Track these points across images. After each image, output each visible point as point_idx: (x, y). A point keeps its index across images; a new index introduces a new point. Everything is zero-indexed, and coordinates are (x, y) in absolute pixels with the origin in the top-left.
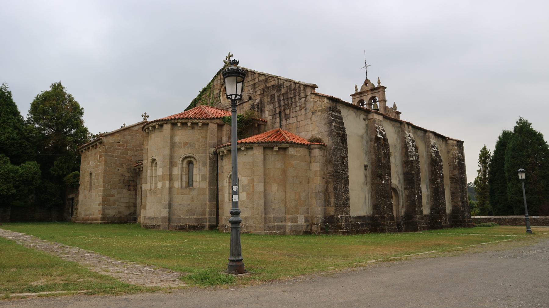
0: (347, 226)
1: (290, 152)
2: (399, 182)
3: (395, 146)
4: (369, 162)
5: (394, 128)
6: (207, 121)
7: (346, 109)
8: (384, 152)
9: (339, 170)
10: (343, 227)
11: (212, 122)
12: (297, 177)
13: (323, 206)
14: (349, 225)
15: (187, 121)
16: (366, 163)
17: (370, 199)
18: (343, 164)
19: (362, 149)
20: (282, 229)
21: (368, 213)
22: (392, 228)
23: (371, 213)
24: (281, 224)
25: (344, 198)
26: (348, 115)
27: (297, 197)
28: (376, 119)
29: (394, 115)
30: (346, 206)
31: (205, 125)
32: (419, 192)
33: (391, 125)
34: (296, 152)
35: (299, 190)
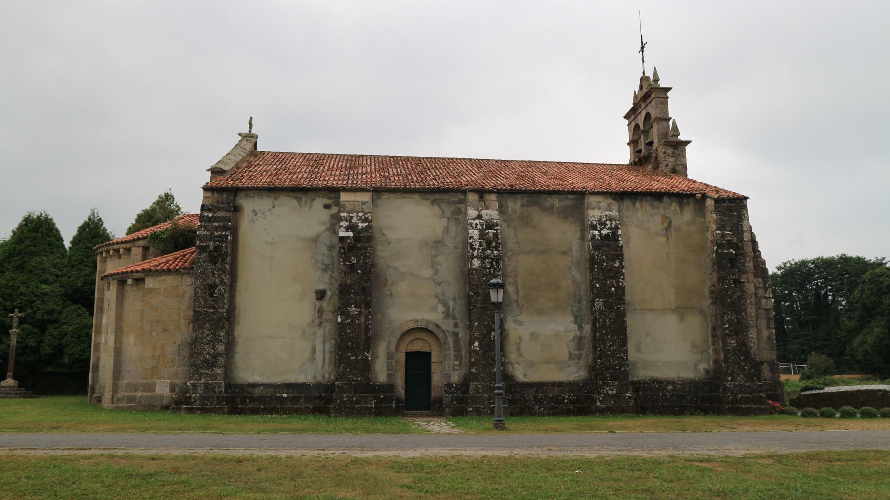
0: (203, 398)
1: (147, 284)
2: (447, 315)
3: (438, 243)
4: (332, 285)
5: (439, 206)
6: (128, 245)
7: (269, 197)
8: (349, 261)
9: (198, 307)
10: (193, 400)
11: (134, 246)
12: (158, 322)
13: (185, 366)
14: (212, 397)
15: (109, 249)
16: (321, 287)
17: (331, 352)
18: (211, 295)
19: (314, 261)
20: (133, 401)
21: (319, 379)
22: (355, 407)
23: (330, 378)
24: (133, 394)
25: (208, 353)
26: (274, 207)
27: (158, 353)
28: (346, 203)
29: (663, 150)
30: (212, 367)
31: (128, 250)
33: (428, 202)
34: (159, 283)
35: (163, 342)
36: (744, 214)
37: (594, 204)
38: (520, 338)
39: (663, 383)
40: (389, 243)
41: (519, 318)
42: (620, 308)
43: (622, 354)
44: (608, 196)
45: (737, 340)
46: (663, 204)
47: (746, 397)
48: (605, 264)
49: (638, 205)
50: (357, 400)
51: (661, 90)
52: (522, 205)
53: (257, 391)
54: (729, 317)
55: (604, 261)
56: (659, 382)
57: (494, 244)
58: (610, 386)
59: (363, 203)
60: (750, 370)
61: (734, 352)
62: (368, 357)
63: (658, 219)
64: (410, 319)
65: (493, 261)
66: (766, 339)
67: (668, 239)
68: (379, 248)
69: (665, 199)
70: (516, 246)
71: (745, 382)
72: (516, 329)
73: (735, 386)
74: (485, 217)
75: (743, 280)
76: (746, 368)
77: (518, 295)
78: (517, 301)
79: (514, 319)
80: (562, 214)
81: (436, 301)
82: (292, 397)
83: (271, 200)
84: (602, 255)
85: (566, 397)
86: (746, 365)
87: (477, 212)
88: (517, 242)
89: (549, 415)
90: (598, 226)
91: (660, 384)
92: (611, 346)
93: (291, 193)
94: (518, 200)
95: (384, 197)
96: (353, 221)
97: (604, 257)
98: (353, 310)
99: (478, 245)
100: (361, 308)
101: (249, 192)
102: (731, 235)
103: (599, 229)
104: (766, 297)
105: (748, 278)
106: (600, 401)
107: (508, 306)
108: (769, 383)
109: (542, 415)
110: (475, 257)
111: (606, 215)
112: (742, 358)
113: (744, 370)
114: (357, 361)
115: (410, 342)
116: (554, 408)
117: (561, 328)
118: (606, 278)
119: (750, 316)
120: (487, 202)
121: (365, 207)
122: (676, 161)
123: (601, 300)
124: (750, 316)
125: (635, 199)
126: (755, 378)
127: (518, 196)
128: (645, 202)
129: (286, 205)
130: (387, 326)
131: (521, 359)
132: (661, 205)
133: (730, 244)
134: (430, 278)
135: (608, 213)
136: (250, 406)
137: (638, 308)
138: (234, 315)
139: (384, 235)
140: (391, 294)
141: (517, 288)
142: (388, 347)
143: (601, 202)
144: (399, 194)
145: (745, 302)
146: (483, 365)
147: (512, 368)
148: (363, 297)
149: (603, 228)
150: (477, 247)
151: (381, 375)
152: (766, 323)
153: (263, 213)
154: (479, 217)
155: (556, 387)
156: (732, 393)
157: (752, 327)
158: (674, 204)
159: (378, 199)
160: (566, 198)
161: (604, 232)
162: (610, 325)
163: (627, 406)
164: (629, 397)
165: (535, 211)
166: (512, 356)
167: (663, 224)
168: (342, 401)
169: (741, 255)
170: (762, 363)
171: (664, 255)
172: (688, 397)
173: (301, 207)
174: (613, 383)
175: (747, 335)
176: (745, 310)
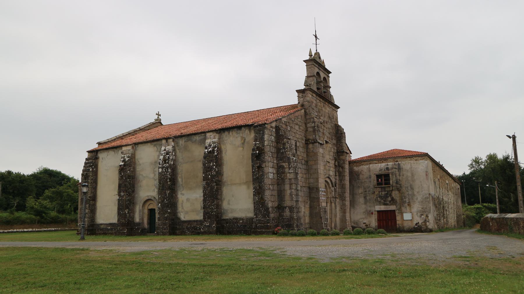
7: (106, 152)
8: (121, 175)
26: (108, 155)
32: (164, 200)
33: (153, 146)
36: (265, 132)
37: (209, 137)
38: (183, 201)
39: (238, 219)
40: (140, 165)
41: (183, 192)
42: (212, 185)
43: (212, 207)
44: (214, 132)
45: (258, 197)
46: (242, 131)
47: (261, 226)
48: (207, 165)
49: (231, 133)
50: (122, 229)
51: (309, 61)
52: (185, 142)
53: (102, 226)
54: (255, 186)
55: (206, 163)
56: (236, 219)
57: (167, 161)
58: (206, 222)
59: (129, 150)
60: (264, 212)
61: (257, 203)
62: (126, 212)
63: (239, 139)
64: (146, 196)
65: (166, 169)
66: (289, 195)
67: (243, 148)
68: (137, 167)
69: (243, 129)
70: (182, 160)
71: (262, 218)
72: (181, 197)
73: (257, 220)
74: (167, 150)
75: (263, 166)
76: (262, 211)
77: (182, 182)
78: (182, 185)
79: (181, 193)
80: (199, 143)
81: (155, 187)
82: (111, 228)
83: (107, 153)
84: (206, 161)
85: (198, 227)
86: (262, 210)
87: (165, 148)
88: (182, 159)
89: (191, 235)
90: (208, 147)
91: (236, 220)
92: (208, 203)
93: (112, 149)
94: (183, 139)
95: (139, 146)
96: (125, 158)
97: (206, 161)
98: (122, 194)
99: (161, 162)
100: (124, 193)
101: (101, 151)
102: (259, 143)
103: (208, 148)
104: (289, 173)
105: (266, 165)
106: (202, 228)
107: (178, 187)
108: (287, 218)
109: (189, 235)
110: (160, 168)
111: (212, 142)
112: (261, 206)
113: (261, 212)
114: (123, 213)
115: (149, 205)
116: (193, 232)
117: (198, 196)
118: (207, 171)
119: (266, 184)
120: (169, 143)
121: (129, 151)
122: (304, 100)
123: (205, 182)
124: (266, 184)
125: (230, 131)
126: (266, 216)
127: (183, 138)
128: (234, 131)
129: (111, 153)
130: (139, 199)
131: (183, 210)
132: (241, 132)
133: (258, 148)
134: (153, 178)
135: (214, 140)
136: (99, 232)
137: (229, 183)
138: (97, 198)
139: (139, 162)
140: (140, 186)
141: (182, 179)
142: (139, 208)
143: (211, 135)
144: (144, 144)
145: (264, 177)
146: (162, 214)
147: (180, 215)
148: (125, 188)
149: (210, 148)
150: (161, 163)
151: (137, 219)
152: (289, 186)
153: (105, 158)
154: (165, 150)
155: (195, 223)
156: (255, 224)
157: (267, 190)
158: (247, 130)
159: (137, 147)
160: (201, 135)
161: (209, 150)
162: (208, 194)
163: (212, 231)
164: (214, 226)
165: (189, 143)
166: (180, 209)
167: (241, 141)
168: (117, 230)
169: (263, 153)
170: (286, 207)
171: (241, 157)
172: (248, 226)
173: (115, 154)
174: (208, 220)
175: (264, 194)
176: (264, 181)
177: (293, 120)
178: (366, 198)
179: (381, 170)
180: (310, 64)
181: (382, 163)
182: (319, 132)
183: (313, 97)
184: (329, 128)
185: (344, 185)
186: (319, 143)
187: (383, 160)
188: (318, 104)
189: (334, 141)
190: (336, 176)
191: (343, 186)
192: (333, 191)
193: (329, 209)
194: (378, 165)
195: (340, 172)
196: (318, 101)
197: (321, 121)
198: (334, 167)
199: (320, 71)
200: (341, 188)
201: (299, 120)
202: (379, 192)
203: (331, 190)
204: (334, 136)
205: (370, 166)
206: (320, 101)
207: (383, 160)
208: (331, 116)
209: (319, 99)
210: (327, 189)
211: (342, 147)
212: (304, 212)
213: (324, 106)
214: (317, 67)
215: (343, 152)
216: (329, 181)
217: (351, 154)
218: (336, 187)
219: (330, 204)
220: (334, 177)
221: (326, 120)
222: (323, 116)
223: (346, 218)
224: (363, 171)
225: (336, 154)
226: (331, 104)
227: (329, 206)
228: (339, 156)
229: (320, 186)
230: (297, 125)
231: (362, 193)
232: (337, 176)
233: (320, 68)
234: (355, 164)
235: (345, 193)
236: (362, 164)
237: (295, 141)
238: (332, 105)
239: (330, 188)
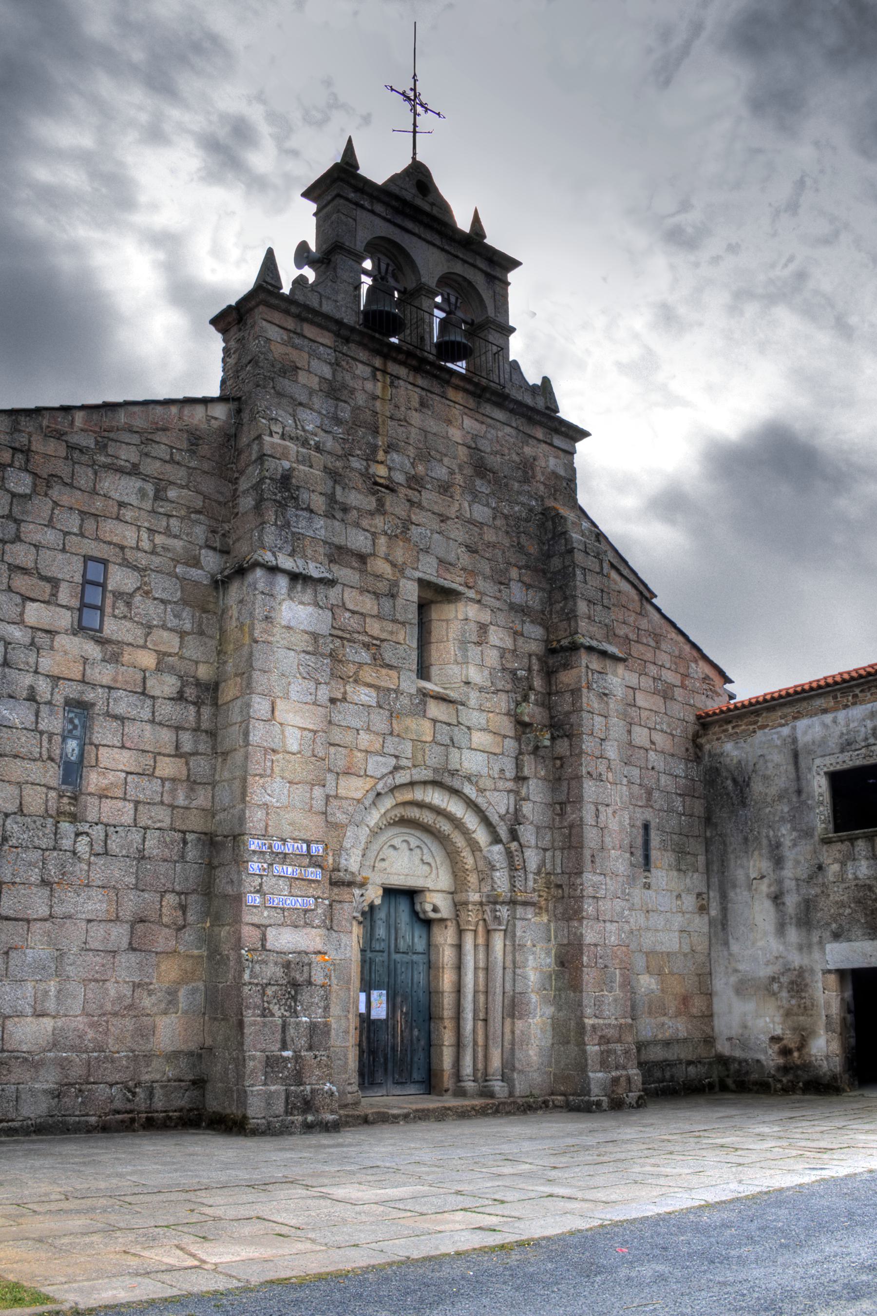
177: (88, 441)
178: (784, 904)
179: (847, 745)
180: (329, 198)
181: (854, 704)
182: (305, 514)
183: (297, 341)
184: (472, 522)
185: (574, 831)
186: (274, 570)
187: (857, 691)
188: (351, 383)
189: (533, 599)
190: (520, 779)
191: (570, 834)
192: (493, 868)
193: (476, 969)
194: (835, 721)
195: (561, 758)
196: (362, 370)
197: (382, 471)
198: (512, 734)
199: (415, 239)
200: (563, 849)
201: (161, 451)
202: (843, 864)
203: (485, 858)
204: (520, 568)
205: (794, 728)
206: (384, 372)
207: (858, 686)
208: (494, 461)
209: (378, 362)
210: (458, 853)
211: (573, 623)
212: (136, 986)
213: (423, 404)
214: (372, 212)
215: (574, 647)
216: (456, 808)
217: (731, 681)
218: (514, 846)
219: (481, 941)
220: (510, 785)
221: (440, 472)
222: (412, 452)
223: (582, 1017)
224: (766, 762)
225: (534, 660)
226: (500, 405)
227: (476, 946)
228: (549, 674)
229: (255, 819)
230: (129, 474)
231: (763, 877)
232: (525, 779)
233: (410, 225)
234: (730, 727)
235: (580, 873)
236: (761, 721)
237: (87, 559)
238: (511, 411)
239: (474, 846)
